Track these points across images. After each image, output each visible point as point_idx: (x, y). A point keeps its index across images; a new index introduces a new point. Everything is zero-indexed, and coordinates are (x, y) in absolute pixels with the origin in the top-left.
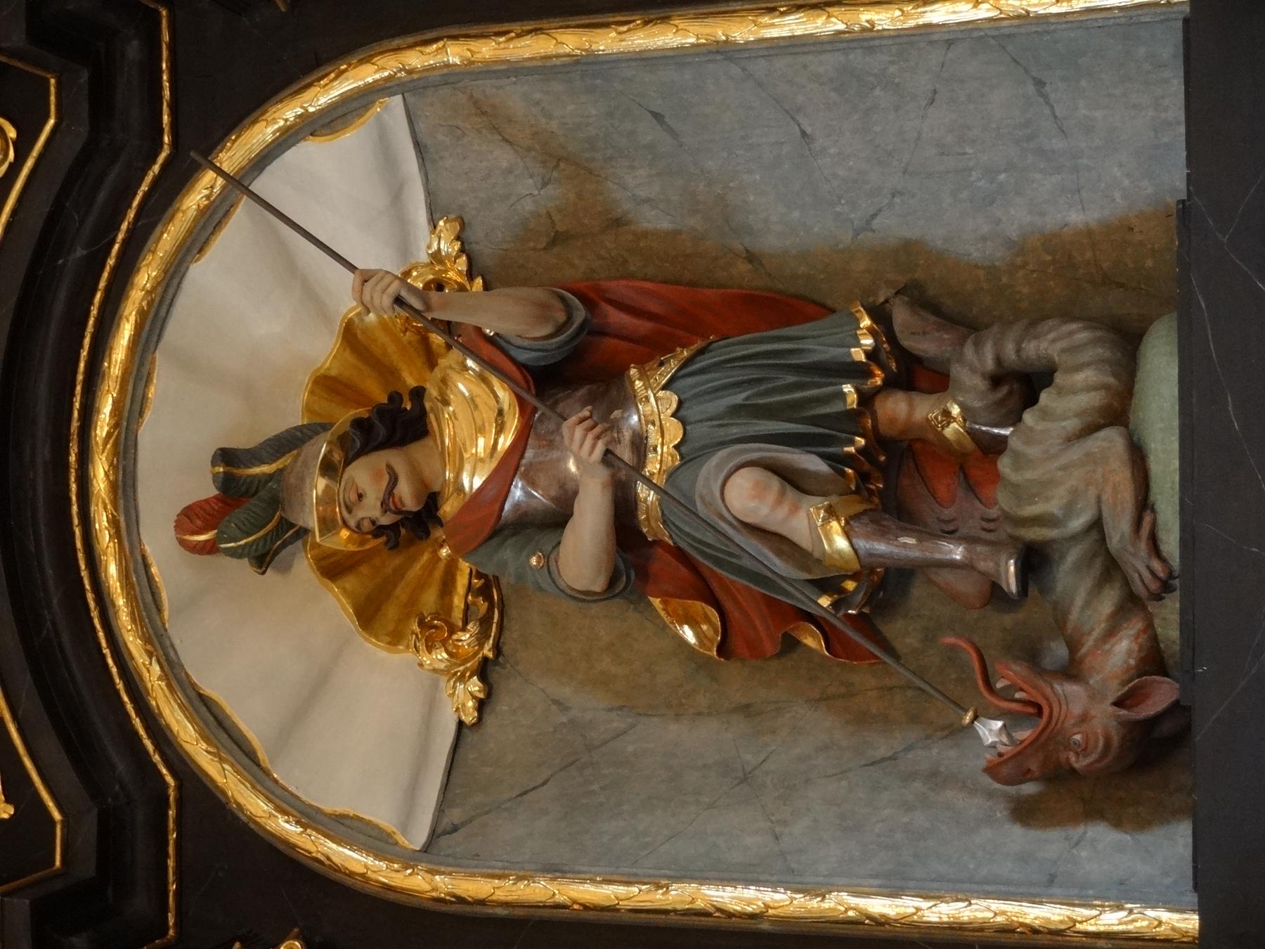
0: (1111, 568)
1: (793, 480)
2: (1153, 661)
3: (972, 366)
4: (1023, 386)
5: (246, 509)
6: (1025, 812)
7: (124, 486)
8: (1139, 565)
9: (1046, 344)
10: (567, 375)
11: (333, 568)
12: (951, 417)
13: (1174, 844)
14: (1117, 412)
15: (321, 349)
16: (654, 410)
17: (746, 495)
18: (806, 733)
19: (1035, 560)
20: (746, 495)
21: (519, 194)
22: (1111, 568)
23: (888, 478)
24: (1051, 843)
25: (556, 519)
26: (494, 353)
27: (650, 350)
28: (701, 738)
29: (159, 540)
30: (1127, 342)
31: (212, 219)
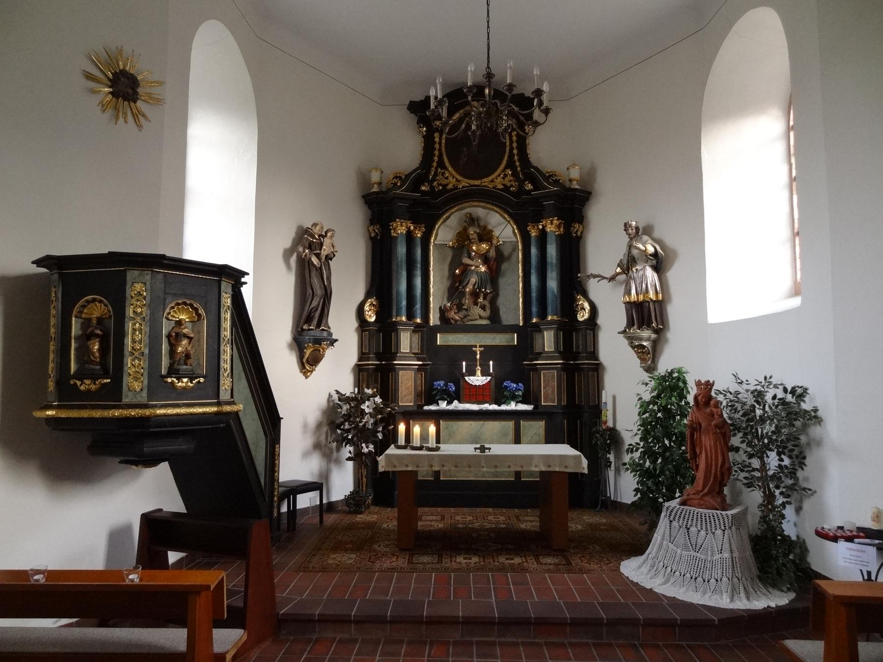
0: (465, 317)
1: (474, 285)
2: (456, 321)
3: (486, 303)
4: (483, 308)
5: (472, 220)
6: (440, 308)
7: (474, 206)
8: (465, 320)
9: (488, 312)
10: (486, 260)
11: (465, 229)
12: (481, 300)
13: (439, 323)
14: (481, 318)
15: (490, 227)
16: (483, 269)
17: (473, 280)
18: (446, 284)
19: (467, 310)
20: (473, 280)
21: (506, 251)
22: (465, 317)
23: (475, 295)
24: (438, 311)
25: (470, 257)
26: (488, 251)
27: (489, 268)
28: (446, 273)
29: (468, 210)
30: (489, 318)
31: (505, 218)
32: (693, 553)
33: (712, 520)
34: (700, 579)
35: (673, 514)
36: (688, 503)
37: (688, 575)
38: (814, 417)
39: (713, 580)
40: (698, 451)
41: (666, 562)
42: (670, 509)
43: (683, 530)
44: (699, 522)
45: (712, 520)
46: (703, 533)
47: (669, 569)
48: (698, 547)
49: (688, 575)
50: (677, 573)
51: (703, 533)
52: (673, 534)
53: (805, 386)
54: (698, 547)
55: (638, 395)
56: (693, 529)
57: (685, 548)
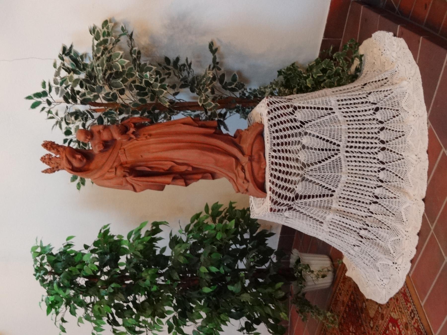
32: (342, 154)
33: (281, 127)
34: (382, 136)
35: (283, 192)
36: (261, 181)
37: (381, 156)
38: (107, 35)
39: (378, 116)
40: (167, 165)
41: (368, 199)
42: (275, 198)
43: (308, 173)
44: (288, 148)
45: (281, 127)
46: (305, 140)
47: (378, 191)
48: (329, 146)
49: (381, 156)
50: (382, 175)
51: (305, 140)
52: (317, 191)
53: (60, 51)
54: (329, 146)
55: (80, 320)
56: (303, 157)
57: (337, 166)
